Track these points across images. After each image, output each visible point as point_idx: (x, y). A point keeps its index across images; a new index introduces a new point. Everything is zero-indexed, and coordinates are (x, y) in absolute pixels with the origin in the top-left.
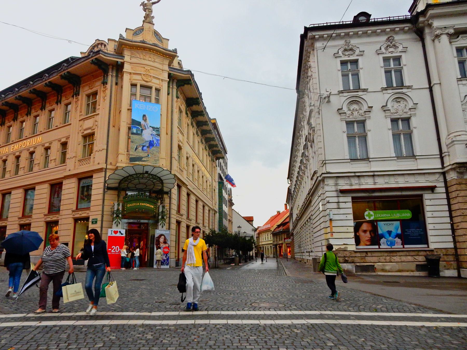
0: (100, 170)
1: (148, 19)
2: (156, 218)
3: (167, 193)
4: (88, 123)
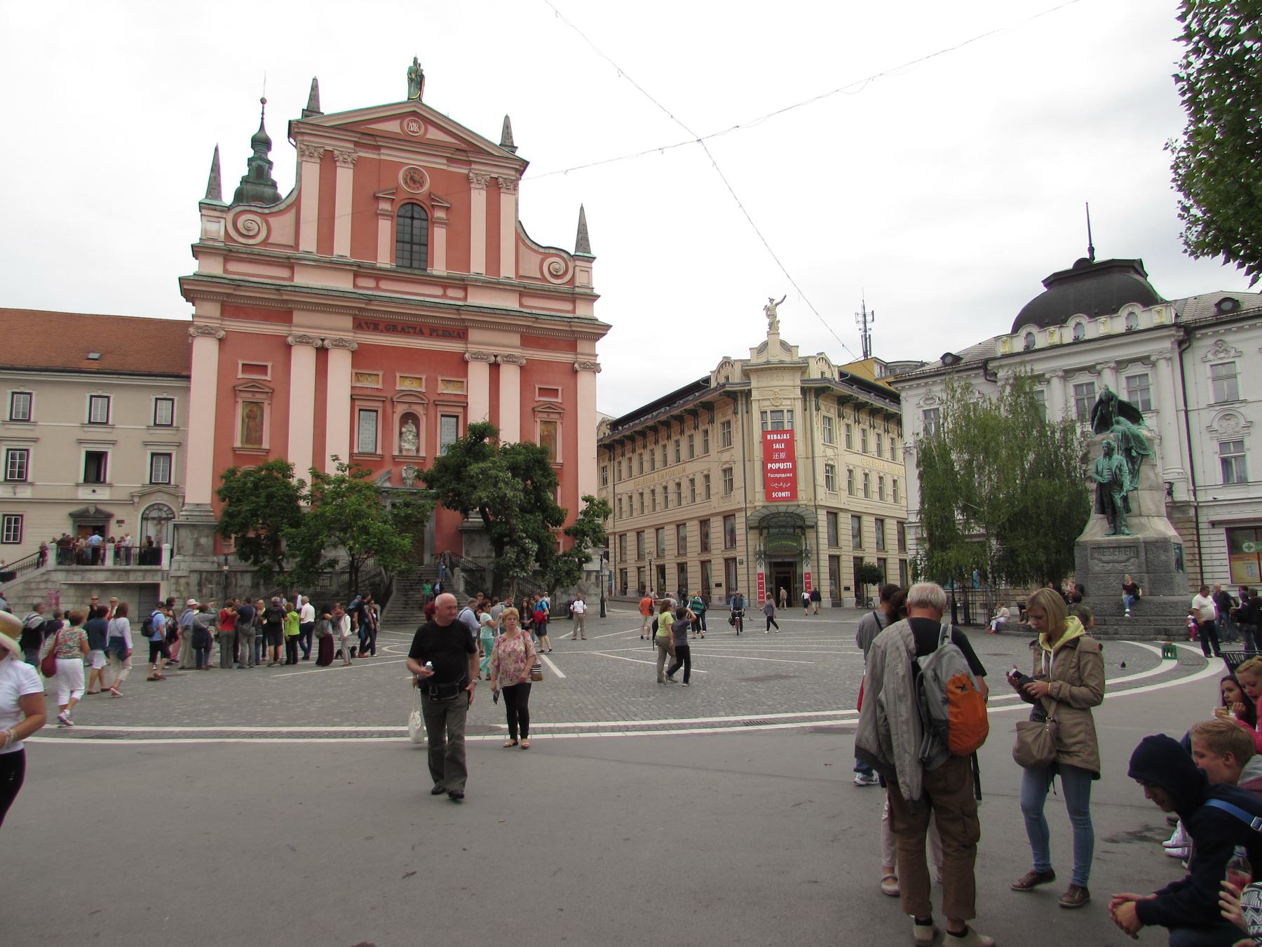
0: (740, 510)
1: (773, 326)
2: (802, 555)
3: (812, 527)
4: (726, 457)
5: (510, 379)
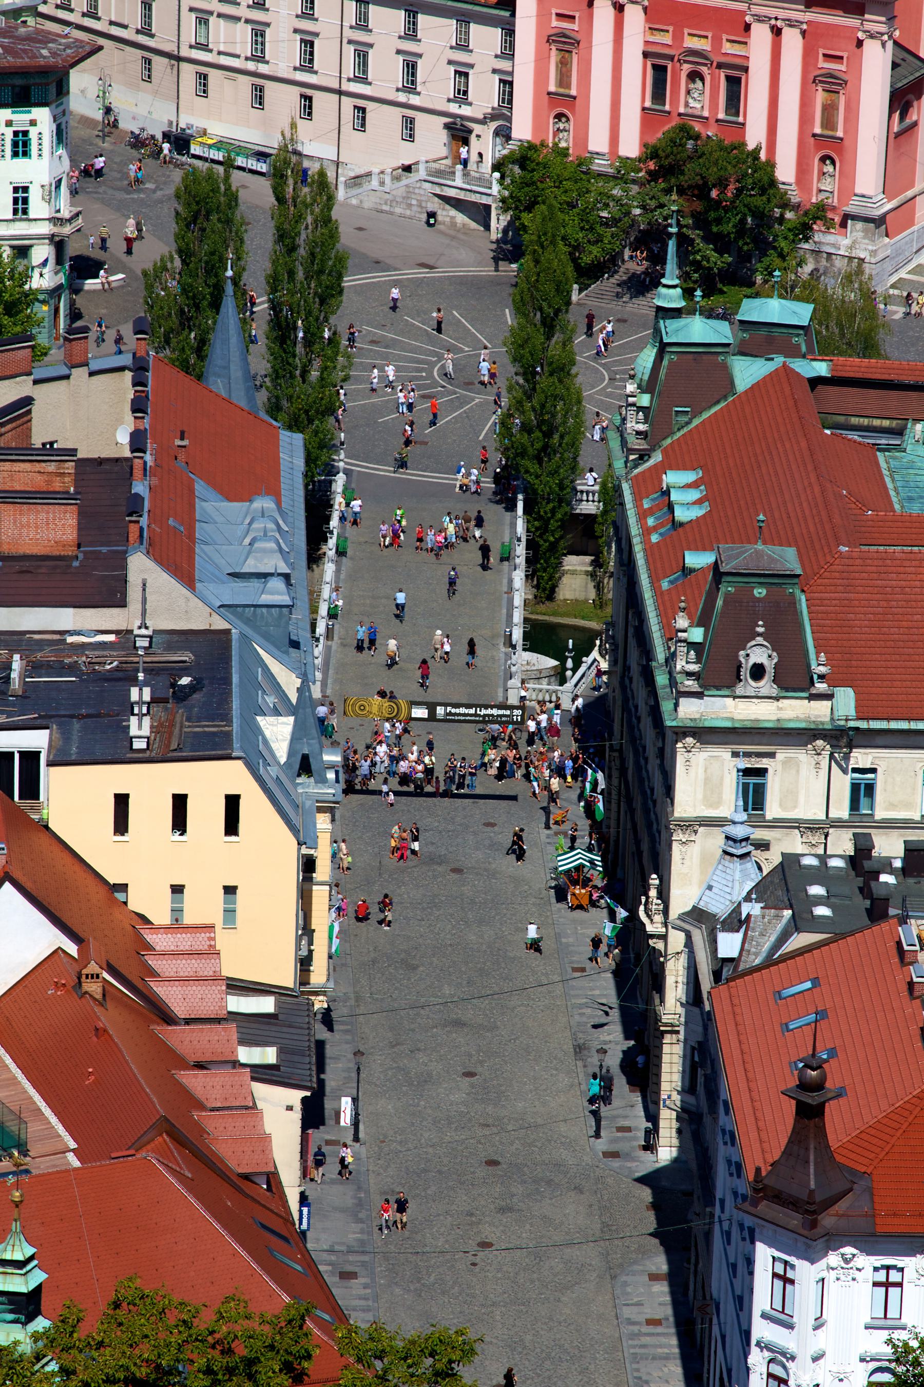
5: (792, 41)
